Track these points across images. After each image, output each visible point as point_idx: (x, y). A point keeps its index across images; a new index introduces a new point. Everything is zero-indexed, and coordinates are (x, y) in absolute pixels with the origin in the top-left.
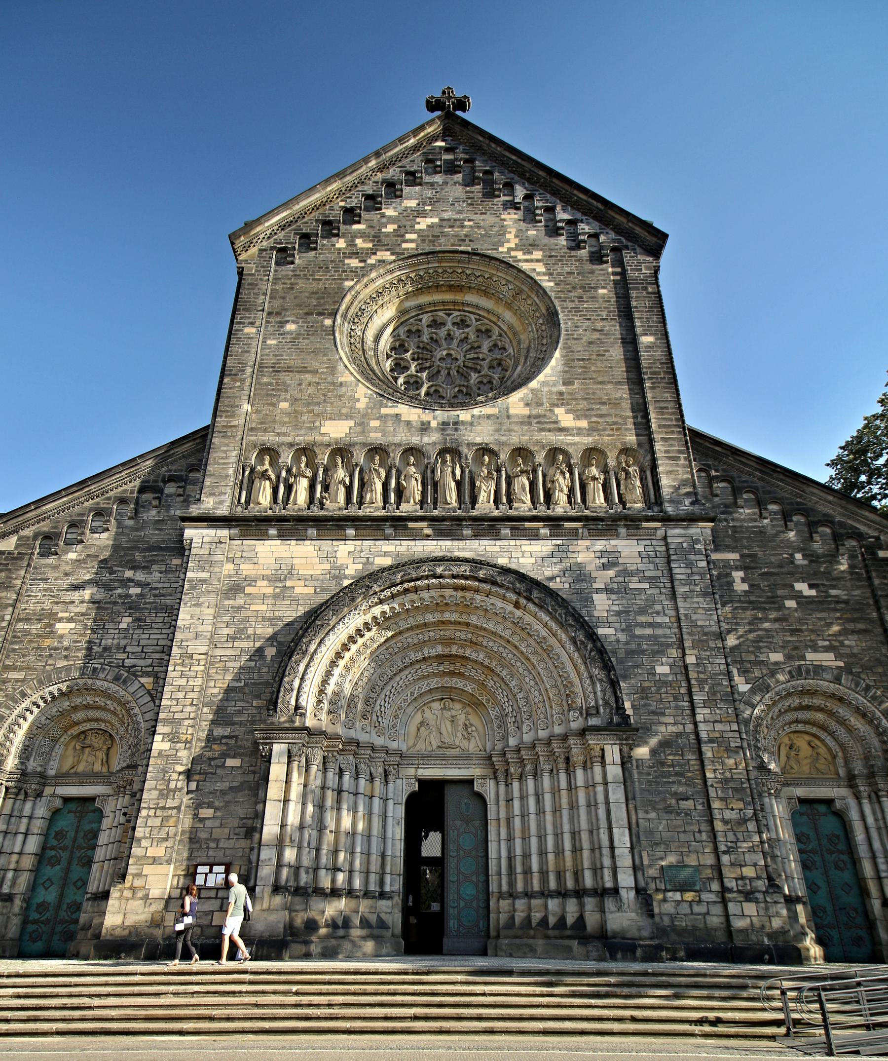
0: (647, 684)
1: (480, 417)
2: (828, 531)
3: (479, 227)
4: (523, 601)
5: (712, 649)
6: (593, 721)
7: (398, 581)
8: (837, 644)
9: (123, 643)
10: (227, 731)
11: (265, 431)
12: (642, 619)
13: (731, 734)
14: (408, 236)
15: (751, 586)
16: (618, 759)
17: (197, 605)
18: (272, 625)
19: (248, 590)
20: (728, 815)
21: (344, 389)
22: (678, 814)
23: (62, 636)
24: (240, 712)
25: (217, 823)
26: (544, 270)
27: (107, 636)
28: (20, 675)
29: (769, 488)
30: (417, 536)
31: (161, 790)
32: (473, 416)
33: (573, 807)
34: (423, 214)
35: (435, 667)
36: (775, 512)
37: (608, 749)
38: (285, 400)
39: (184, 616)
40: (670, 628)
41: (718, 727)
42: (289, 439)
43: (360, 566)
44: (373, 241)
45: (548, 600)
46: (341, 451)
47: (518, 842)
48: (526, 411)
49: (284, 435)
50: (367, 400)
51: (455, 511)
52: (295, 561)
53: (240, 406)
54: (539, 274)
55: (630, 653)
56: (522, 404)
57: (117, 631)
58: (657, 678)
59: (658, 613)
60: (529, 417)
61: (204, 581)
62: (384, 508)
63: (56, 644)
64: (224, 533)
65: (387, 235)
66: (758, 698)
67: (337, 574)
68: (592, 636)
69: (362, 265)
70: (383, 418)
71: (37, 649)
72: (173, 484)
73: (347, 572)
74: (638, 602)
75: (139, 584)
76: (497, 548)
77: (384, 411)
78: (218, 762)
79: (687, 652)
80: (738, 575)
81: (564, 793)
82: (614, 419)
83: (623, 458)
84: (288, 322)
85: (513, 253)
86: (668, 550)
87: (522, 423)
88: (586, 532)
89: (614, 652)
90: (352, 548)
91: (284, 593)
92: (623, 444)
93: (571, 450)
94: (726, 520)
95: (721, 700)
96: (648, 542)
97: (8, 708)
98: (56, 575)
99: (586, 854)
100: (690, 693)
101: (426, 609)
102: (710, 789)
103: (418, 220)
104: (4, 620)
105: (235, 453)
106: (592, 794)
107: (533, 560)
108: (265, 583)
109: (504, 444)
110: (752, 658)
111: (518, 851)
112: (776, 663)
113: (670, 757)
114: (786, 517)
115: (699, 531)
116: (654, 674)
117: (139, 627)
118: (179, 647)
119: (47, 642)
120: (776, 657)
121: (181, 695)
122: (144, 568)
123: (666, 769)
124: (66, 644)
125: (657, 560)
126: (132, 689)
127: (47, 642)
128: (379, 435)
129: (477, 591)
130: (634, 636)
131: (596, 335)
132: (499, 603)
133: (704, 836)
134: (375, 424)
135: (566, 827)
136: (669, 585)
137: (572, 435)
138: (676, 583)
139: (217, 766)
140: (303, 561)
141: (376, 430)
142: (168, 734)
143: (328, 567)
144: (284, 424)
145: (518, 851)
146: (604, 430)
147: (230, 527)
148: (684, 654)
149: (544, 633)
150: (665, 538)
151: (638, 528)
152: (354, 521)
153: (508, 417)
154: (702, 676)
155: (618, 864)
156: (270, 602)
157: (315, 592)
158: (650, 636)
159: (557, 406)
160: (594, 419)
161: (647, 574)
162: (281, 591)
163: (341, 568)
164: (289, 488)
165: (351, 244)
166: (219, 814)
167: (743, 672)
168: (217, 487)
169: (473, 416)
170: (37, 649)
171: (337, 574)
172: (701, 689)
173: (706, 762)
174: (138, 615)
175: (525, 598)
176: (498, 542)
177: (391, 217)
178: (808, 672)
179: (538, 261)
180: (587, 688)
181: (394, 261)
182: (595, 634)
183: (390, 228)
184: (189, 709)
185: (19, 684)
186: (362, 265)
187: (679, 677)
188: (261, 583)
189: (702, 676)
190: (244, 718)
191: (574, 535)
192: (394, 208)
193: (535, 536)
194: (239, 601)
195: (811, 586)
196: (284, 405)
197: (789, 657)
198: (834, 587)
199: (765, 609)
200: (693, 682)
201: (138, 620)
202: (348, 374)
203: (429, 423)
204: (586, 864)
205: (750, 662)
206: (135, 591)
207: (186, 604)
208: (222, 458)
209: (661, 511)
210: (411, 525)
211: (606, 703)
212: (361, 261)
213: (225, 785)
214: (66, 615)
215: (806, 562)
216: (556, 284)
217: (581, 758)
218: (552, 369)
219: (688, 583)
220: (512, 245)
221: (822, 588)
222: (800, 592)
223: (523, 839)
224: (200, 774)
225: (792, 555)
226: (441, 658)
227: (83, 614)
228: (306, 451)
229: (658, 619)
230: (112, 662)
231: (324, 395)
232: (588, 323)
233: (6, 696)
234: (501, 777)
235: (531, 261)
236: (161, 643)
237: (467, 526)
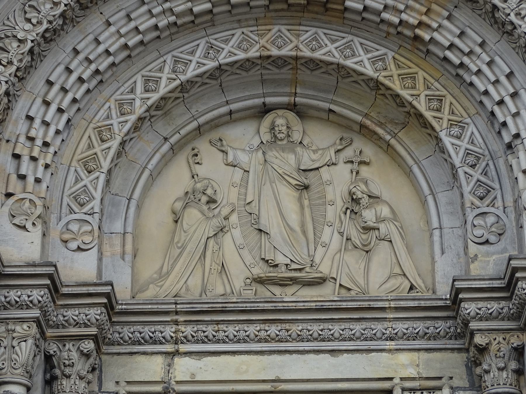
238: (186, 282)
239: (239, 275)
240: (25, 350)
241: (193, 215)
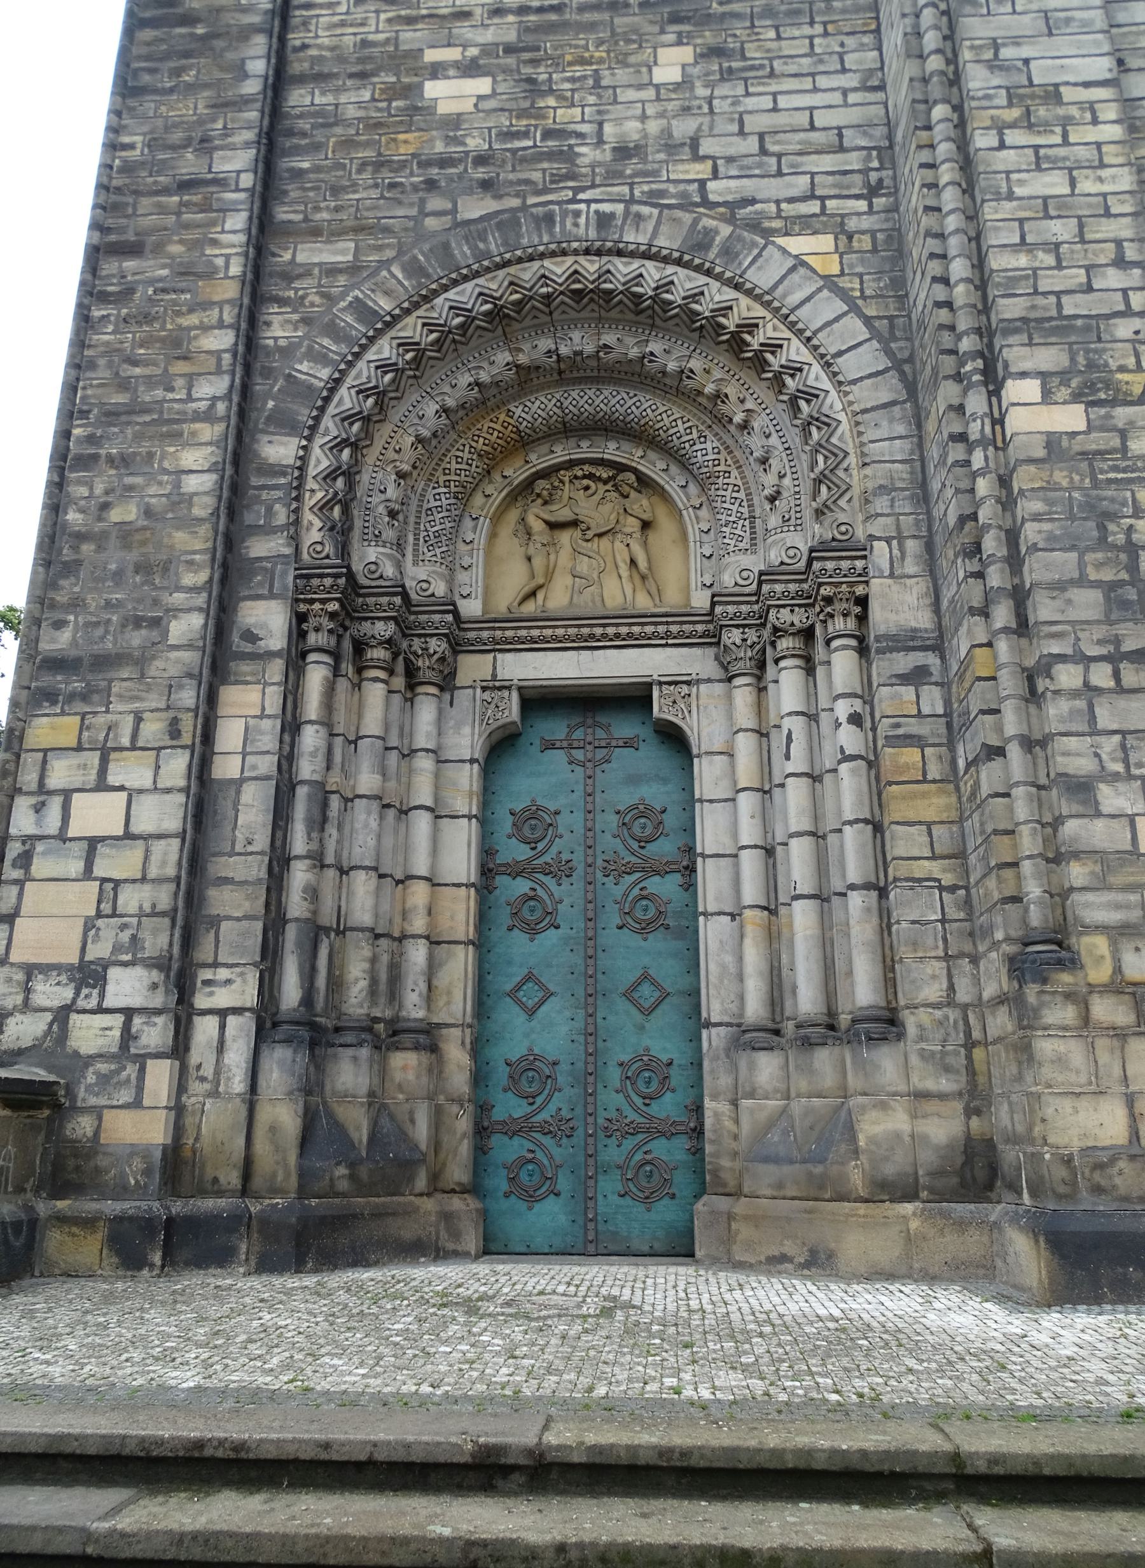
9: (683, 128)
23: (455, 122)
27: (617, 111)
28: (340, 253)
31: (1110, 588)
57: (650, 93)
63: (439, 147)
71: (379, 164)
97: (321, 358)
104: (246, 76)
117: (727, 75)
118: (995, 65)
119: (408, 144)
121: (1061, 230)
124: (475, 143)
127: (408, 144)
142: (1064, 376)
170: (379, 164)
174: (709, 37)
184: (1113, 278)
185: (342, 280)
201: (717, 52)
214: (452, 54)
227: (509, 49)
230: (662, 194)
233: (306, 321)
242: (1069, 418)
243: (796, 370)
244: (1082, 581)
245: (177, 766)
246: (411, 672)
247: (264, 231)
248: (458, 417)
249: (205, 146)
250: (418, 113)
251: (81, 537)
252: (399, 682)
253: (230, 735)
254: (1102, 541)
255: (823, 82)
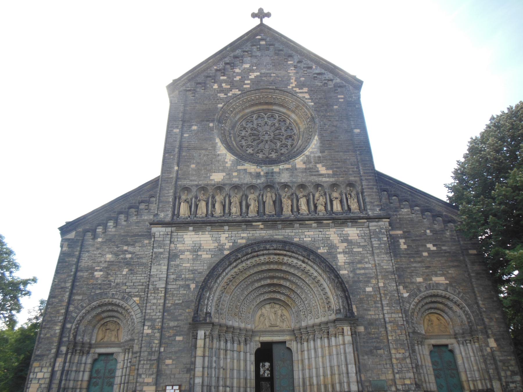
0: (362, 297)
1: (283, 169)
2: (441, 219)
3: (278, 77)
4: (306, 260)
5: (390, 279)
6: (339, 316)
7: (250, 252)
8: (445, 272)
9: (125, 281)
10: (176, 323)
11: (185, 179)
12: (359, 266)
13: (399, 319)
14: (246, 82)
15: (408, 246)
16: (350, 333)
17: (159, 265)
18: (193, 273)
19: (181, 257)
20: (398, 356)
21: (220, 157)
22: (377, 356)
23: (97, 278)
24: (181, 315)
25: (174, 366)
26: (309, 97)
28: (80, 297)
29: (414, 199)
30: (256, 228)
32: (280, 169)
33: (330, 355)
34: (253, 71)
35: (267, 289)
36: (418, 211)
37: (345, 328)
38: (193, 164)
39: (154, 271)
40: (372, 269)
41: (394, 315)
42: (196, 183)
43: (231, 244)
44: (229, 85)
45: (317, 259)
46: (219, 188)
47: (307, 371)
48: (304, 166)
49: (194, 181)
50: (231, 162)
51: (273, 216)
52: (202, 242)
53: (173, 168)
54: (306, 99)
55: (354, 282)
56: (302, 163)
58: (367, 293)
59: (366, 263)
60: (305, 169)
61: (161, 253)
62: (241, 215)
64: (169, 229)
65: (237, 81)
66: (412, 300)
67: (221, 248)
68: (337, 276)
69: (226, 96)
70: (238, 171)
71: (87, 284)
72: (143, 204)
73: (226, 247)
74: (358, 258)
75: (130, 253)
76: (293, 234)
77: (239, 167)
78: (173, 338)
79: (379, 281)
80: (402, 241)
81: (327, 348)
82: (344, 169)
83: (348, 188)
84: (193, 125)
85: (294, 89)
86: (370, 233)
87: (302, 172)
88: (333, 224)
89: (347, 282)
90: (227, 236)
91: (197, 258)
92: (349, 181)
93: (325, 185)
94: (396, 215)
95: (395, 303)
96: (361, 229)
97: (76, 313)
98: (93, 249)
99: (337, 376)
100: (381, 300)
101: (263, 264)
102: (390, 344)
103: (250, 74)
104: (71, 271)
105: (172, 191)
106: (339, 349)
107: (310, 239)
108: (188, 253)
109: (294, 182)
110: (409, 280)
111: (307, 375)
112: (420, 283)
113: (373, 330)
114: (423, 212)
115: (383, 223)
116: (365, 292)
117: (131, 273)
118: (153, 285)
120: (419, 280)
122: (132, 245)
123: (371, 336)
124: (99, 282)
125: (366, 238)
126: (130, 303)
127: (91, 281)
128: (237, 179)
129: (285, 255)
130: (356, 274)
131: (334, 129)
132: (295, 261)
133: (388, 366)
134: (235, 174)
135: (328, 364)
136: (371, 249)
137: (325, 177)
138: (374, 248)
139: (172, 340)
140: (205, 242)
141: (236, 177)
143: (217, 245)
144: (193, 175)
145: (307, 375)
146: (340, 174)
147: (172, 227)
148: (378, 282)
149: (316, 274)
150: (368, 227)
151: (356, 222)
152: (227, 222)
153: (296, 169)
154: (386, 292)
155: (351, 380)
156: (191, 262)
157: (212, 257)
158: (363, 273)
159: (318, 163)
160: (335, 169)
161: (362, 244)
162: (196, 257)
163: (223, 245)
164: (197, 206)
165: (220, 86)
166: (174, 362)
167: (405, 287)
168: (165, 208)
169: (280, 169)
171: (221, 248)
172: (386, 298)
173: (389, 332)
174: (130, 268)
175: (307, 259)
176: (294, 231)
177: (238, 73)
178: (433, 286)
179: (306, 93)
180: (335, 301)
181: (240, 94)
182: (338, 274)
183: (238, 78)
184: (158, 314)
186: (226, 96)
187: (376, 293)
188: (187, 253)
189: (386, 292)
190: (183, 317)
191: (328, 226)
192: (239, 68)
193: (310, 227)
194: (178, 262)
195: (434, 245)
196: (193, 166)
197: (425, 280)
198: (444, 245)
199: (414, 257)
200: (382, 295)
202: (222, 150)
203: (260, 173)
204: (337, 381)
205: (408, 282)
206: (129, 256)
207: (154, 264)
208: (167, 193)
209: (366, 214)
210: (254, 224)
211: (344, 307)
212: (225, 95)
213: (176, 349)
214: (99, 268)
215: (431, 234)
216: (315, 104)
217: (334, 333)
218: (315, 145)
219: (379, 248)
220: (294, 85)
221: (439, 246)
222: (429, 248)
223: (309, 369)
224: (165, 344)
225: (425, 231)
226: (269, 285)
228: (203, 189)
229: (367, 266)
231: (211, 161)
232: (330, 123)
234: (299, 340)
235: (302, 93)
236: (142, 281)
237: (279, 224)
238: (261, 327)
239: (268, 324)
240: (243, 339)
241: (261, 318)
242: (150, 331)
243: (132, 316)
244: (146, 351)
245: (50, 369)
246: (83, 352)
247: (71, 294)
248: (94, 317)
249: (65, 282)
250: (93, 277)
251: (43, 338)
252: (81, 354)
253: (57, 364)
254: (149, 347)
255: (143, 275)
